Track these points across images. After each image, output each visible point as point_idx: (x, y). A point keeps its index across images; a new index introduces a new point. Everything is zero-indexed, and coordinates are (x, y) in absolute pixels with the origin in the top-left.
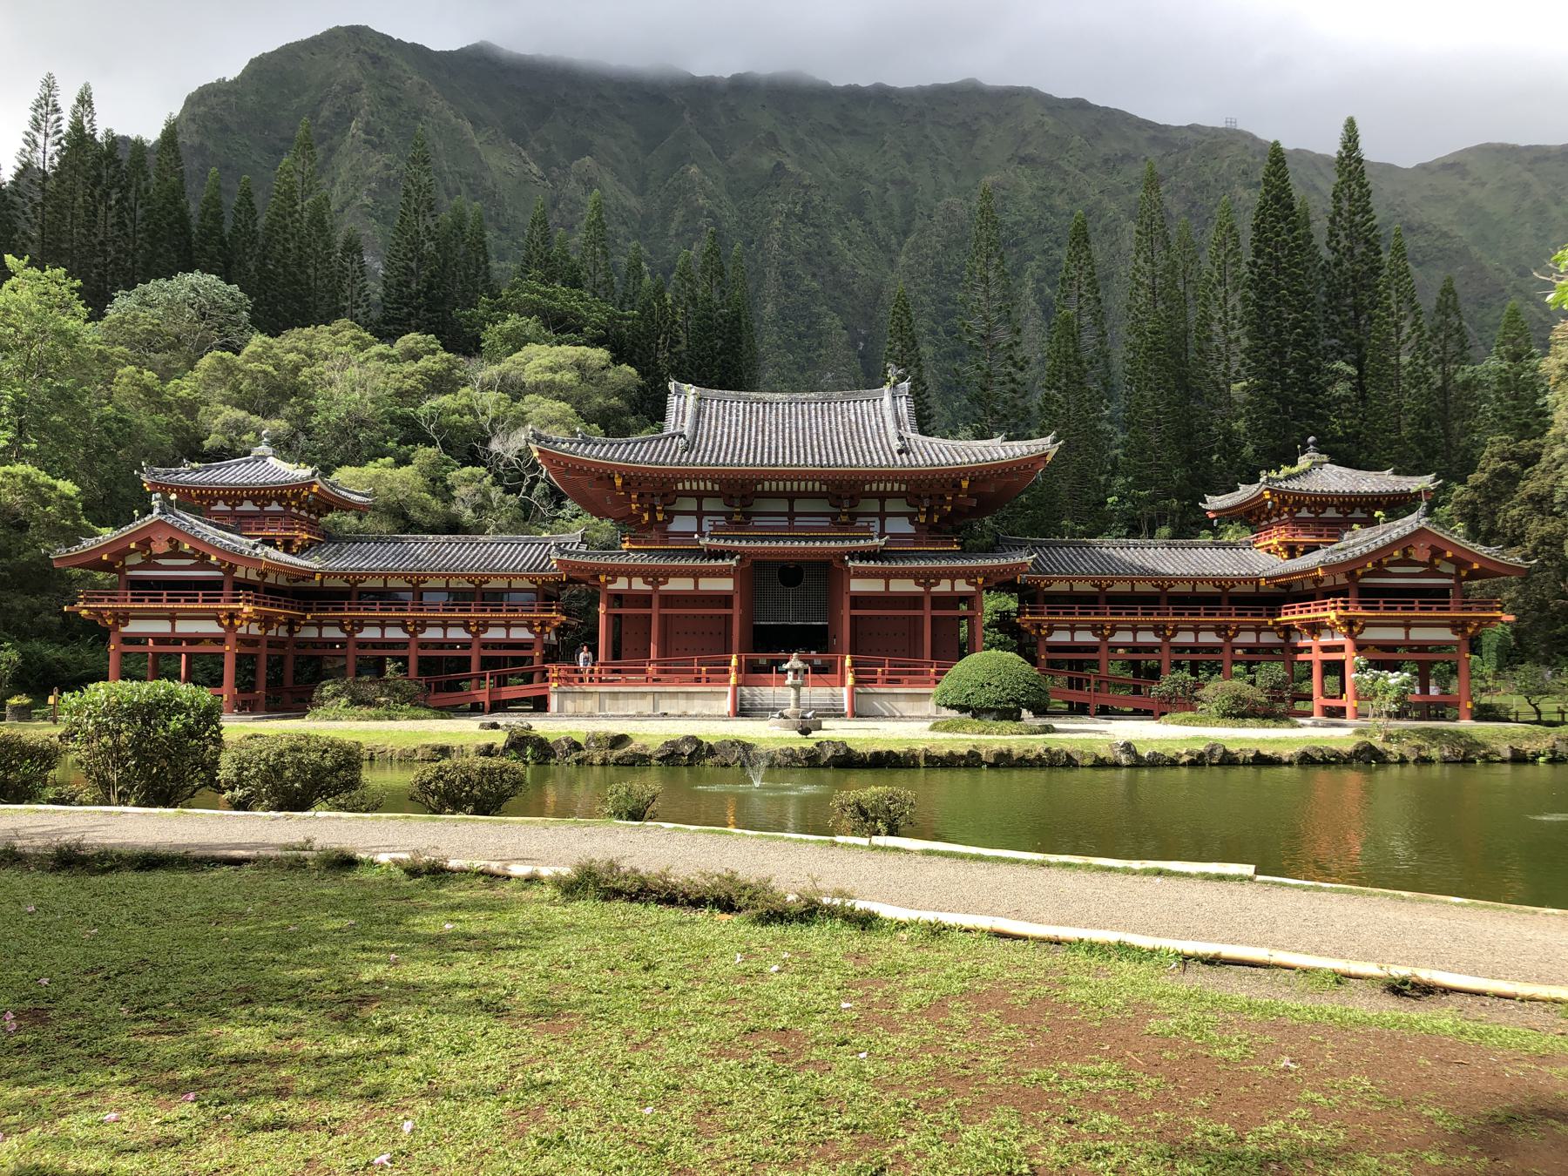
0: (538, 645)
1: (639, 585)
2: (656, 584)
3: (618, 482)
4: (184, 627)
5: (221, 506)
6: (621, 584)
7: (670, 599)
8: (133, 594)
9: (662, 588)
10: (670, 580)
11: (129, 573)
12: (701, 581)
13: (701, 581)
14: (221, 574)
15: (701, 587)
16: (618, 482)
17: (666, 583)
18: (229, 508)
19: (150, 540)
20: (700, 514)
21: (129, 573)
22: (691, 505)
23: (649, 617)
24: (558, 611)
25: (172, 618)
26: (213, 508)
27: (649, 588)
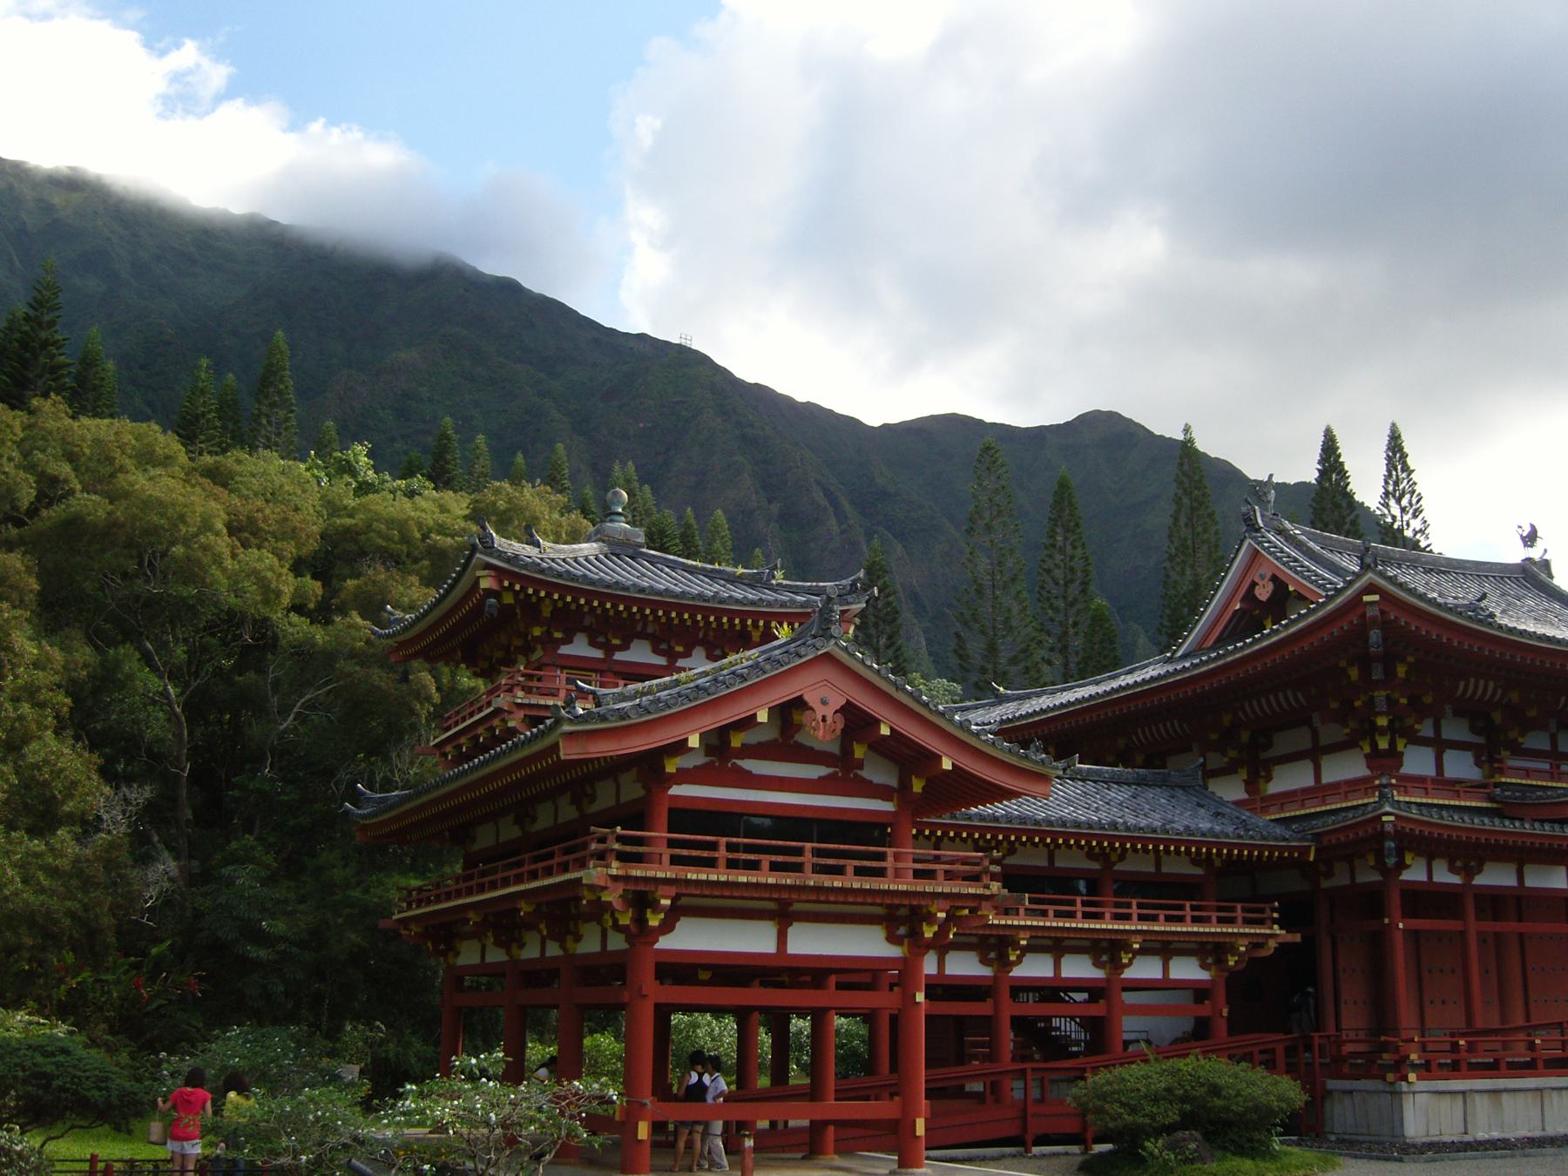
0: (1221, 993)
1: (1444, 876)
2: (1469, 873)
3: (1401, 670)
4: (808, 942)
5: (580, 648)
6: (1415, 873)
7: (1493, 902)
8: (731, 847)
9: (1479, 880)
10: (1487, 867)
11: (675, 790)
12: (1529, 870)
13: (1528, 869)
14: (888, 807)
15: (1529, 883)
16: (1401, 670)
17: (1480, 871)
18: (598, 654)
19: (795, 706)
20: (1440, 746)
21: (675, 790)
22: (1426, 730)
23: (1463, 934)
24: (1275, 921)
25: (783, 914)
26: (565, 650)
27: (1456, 880)
